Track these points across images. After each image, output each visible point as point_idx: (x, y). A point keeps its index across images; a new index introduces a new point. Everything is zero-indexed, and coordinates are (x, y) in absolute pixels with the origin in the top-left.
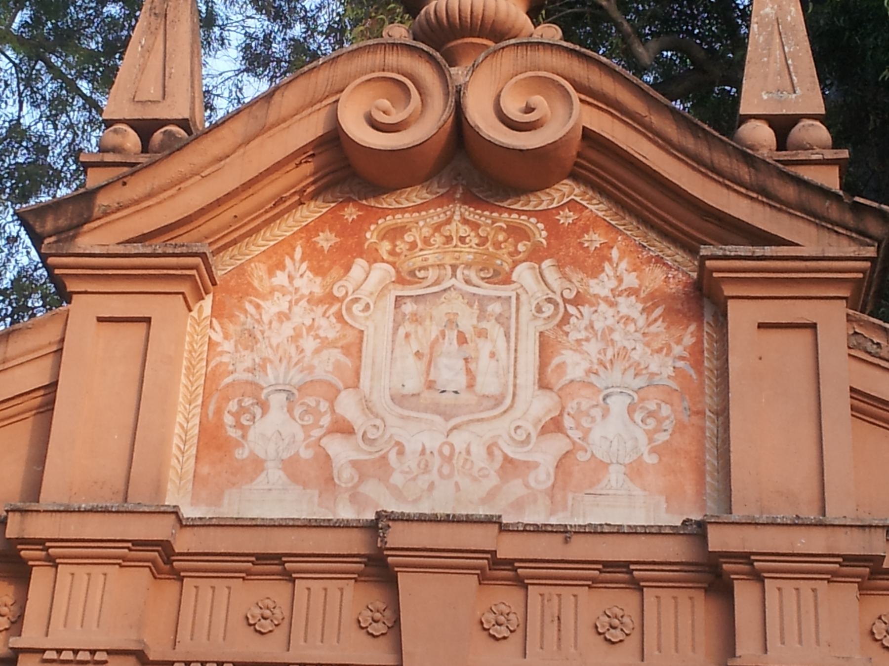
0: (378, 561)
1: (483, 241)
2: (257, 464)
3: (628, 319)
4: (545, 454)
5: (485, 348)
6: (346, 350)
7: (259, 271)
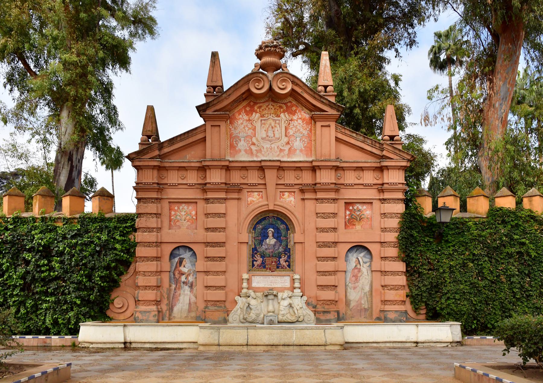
0: (261, 168)
1: (275, 109)
2: (240, 151)
3: (300, 124)
4: (287, 148)
5: (276, 129)
6: (253, 130)
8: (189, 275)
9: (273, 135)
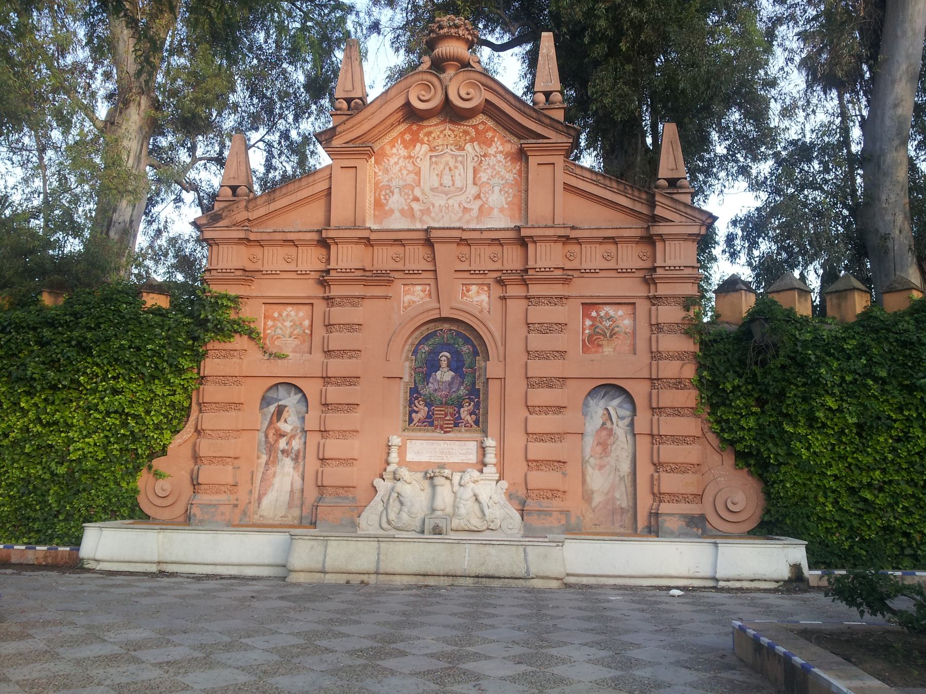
0: (428, 240)
2: (392, 211)
3: (500, 161)
4: (476, 205)
5: (457, 172)
6: (416, 174)
7: (388, 148)
8: (293, 437)
9: (451, 183)
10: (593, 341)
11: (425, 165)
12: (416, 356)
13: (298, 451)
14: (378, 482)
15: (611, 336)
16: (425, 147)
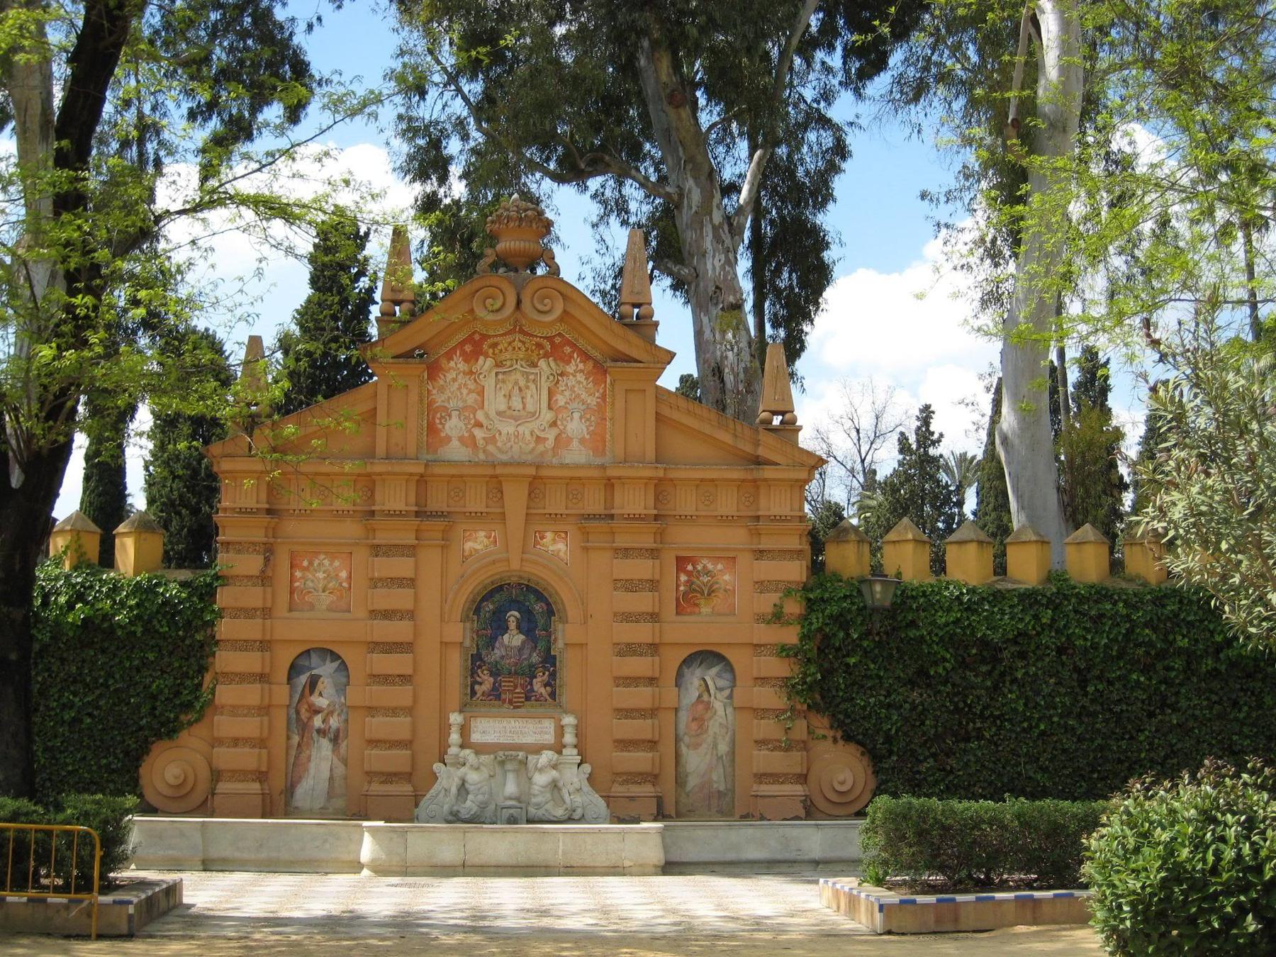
1: (527, 349)
2: (449, 439)
3: (579, 382)
4: (551, 435)
6: (478, 394)
7: (444, 362)
8: (331, 713)
9: (521, 406)
10: (687, 602)
11: (489, 383)
12: (479, 616)
13: (338, 730)
14: (437, 767)
15: (709, 594)
16: (490, 362)
